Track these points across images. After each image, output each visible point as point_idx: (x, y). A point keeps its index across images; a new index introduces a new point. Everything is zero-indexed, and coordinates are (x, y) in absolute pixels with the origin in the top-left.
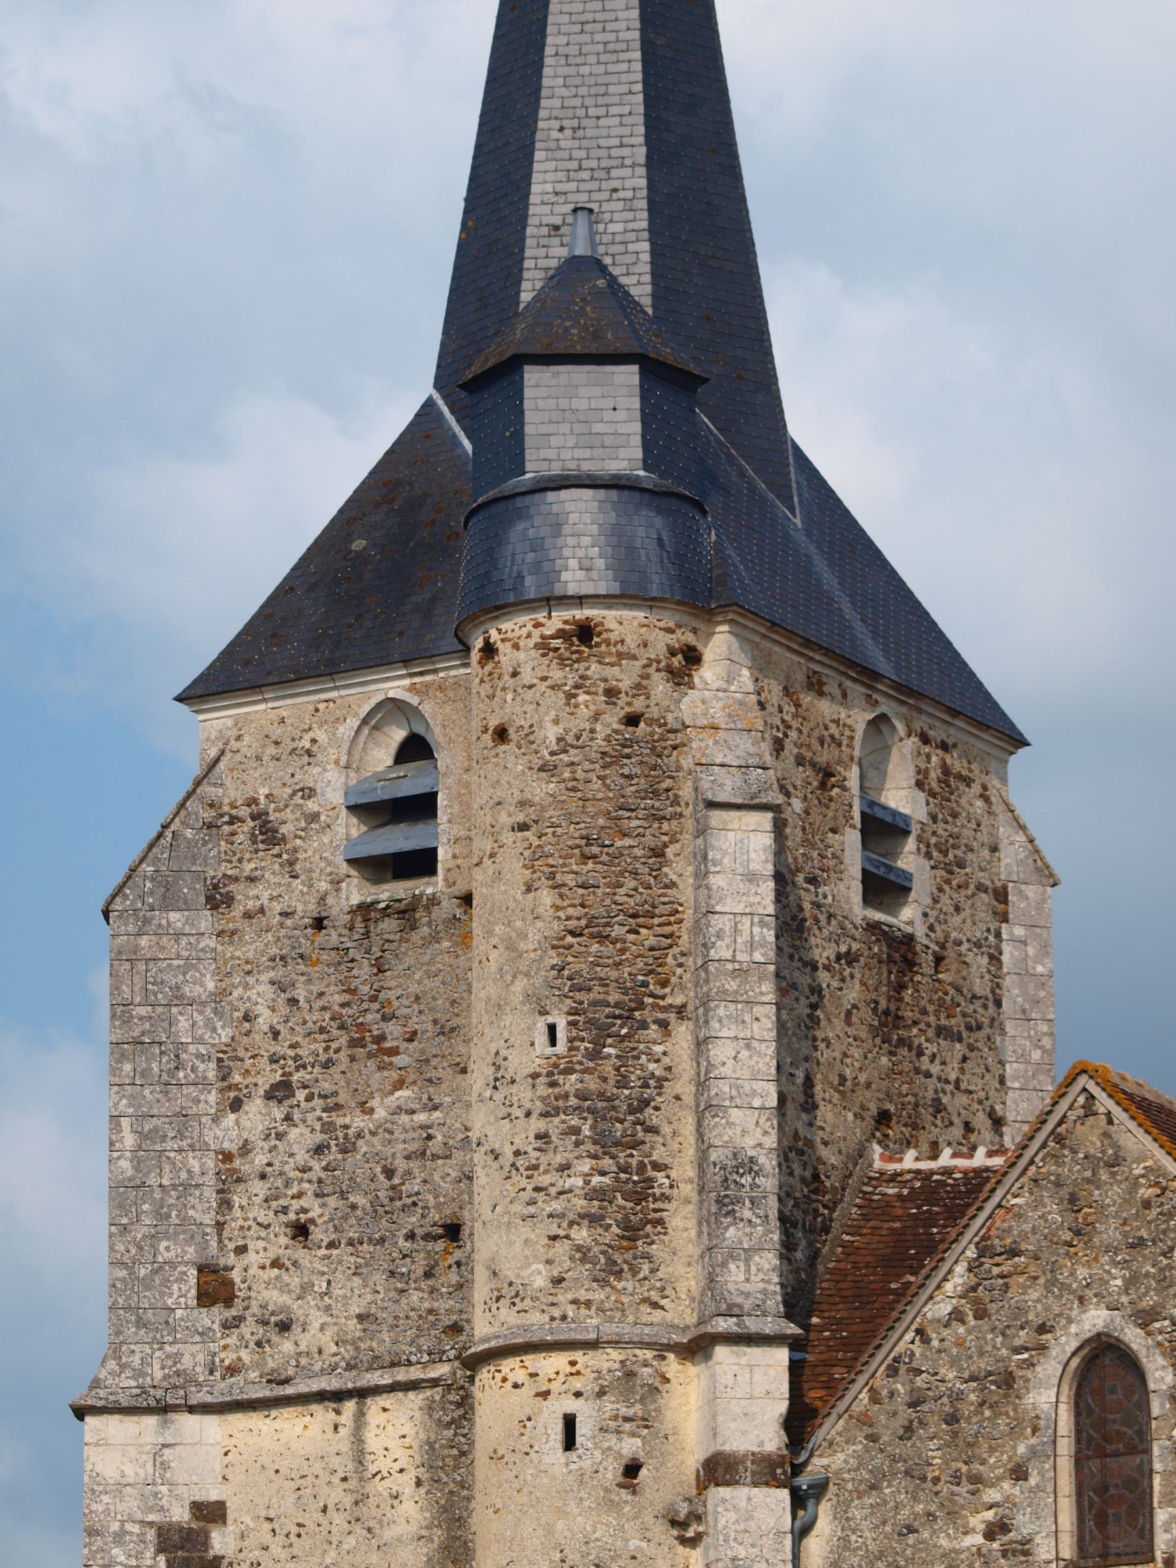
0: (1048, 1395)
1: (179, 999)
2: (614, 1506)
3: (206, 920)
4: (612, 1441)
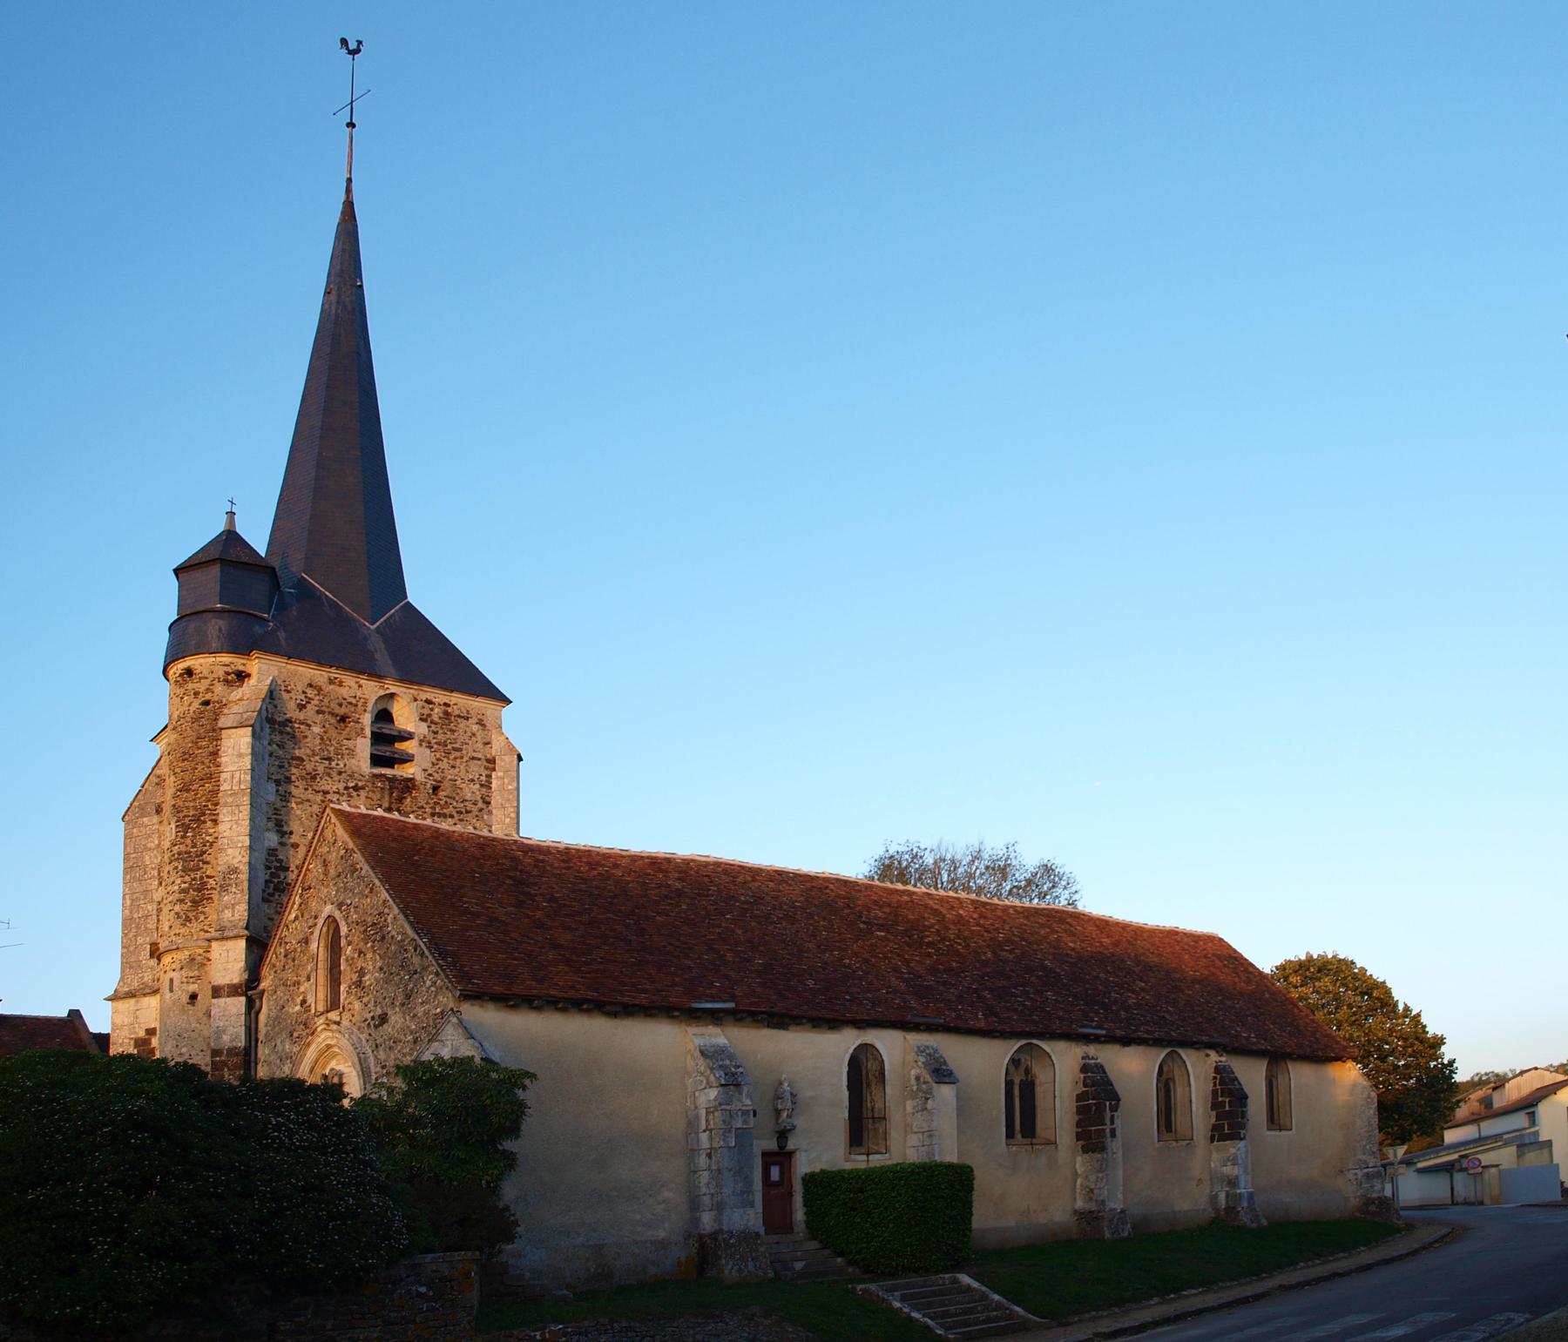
0: (317, 946)
1: (146, 849)
2: (183, 1011)
3: (156, 819)
4: (185, 986)
